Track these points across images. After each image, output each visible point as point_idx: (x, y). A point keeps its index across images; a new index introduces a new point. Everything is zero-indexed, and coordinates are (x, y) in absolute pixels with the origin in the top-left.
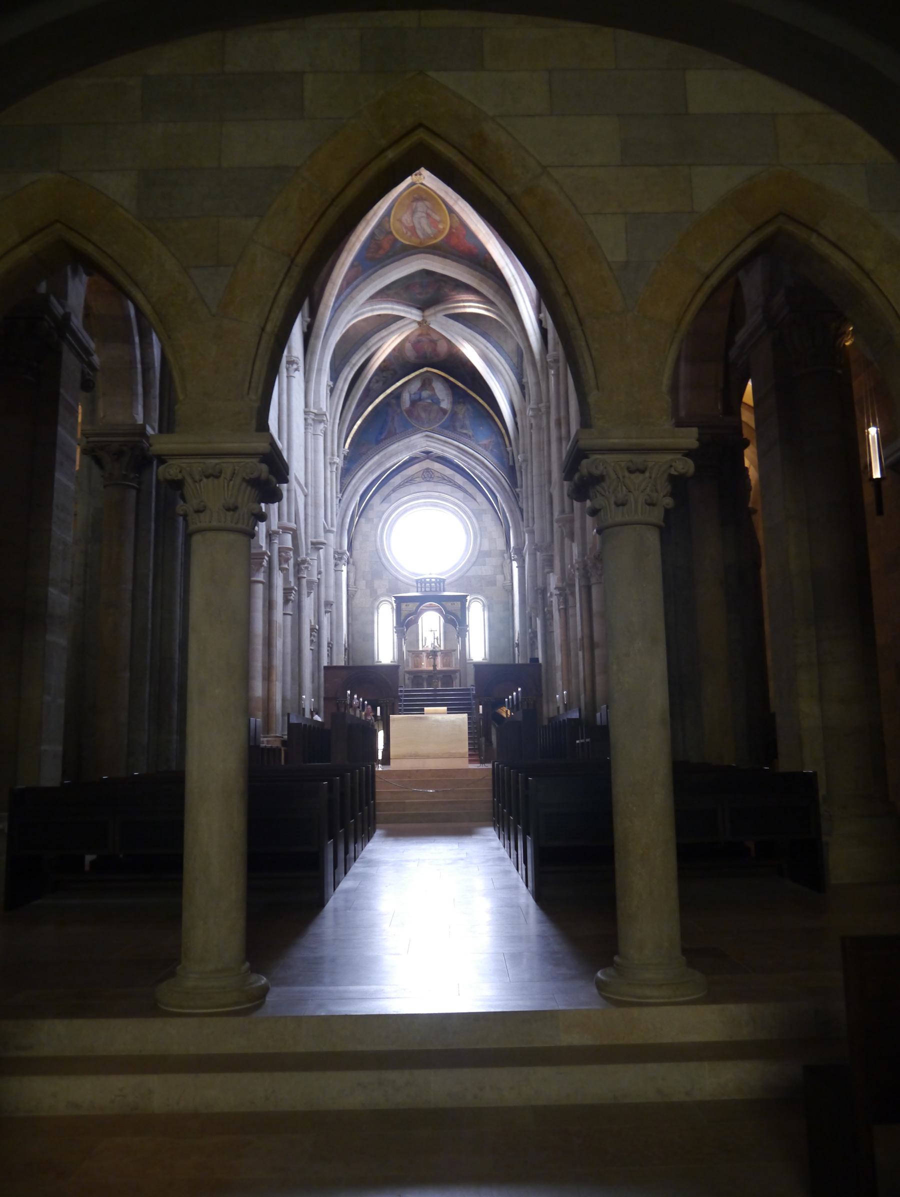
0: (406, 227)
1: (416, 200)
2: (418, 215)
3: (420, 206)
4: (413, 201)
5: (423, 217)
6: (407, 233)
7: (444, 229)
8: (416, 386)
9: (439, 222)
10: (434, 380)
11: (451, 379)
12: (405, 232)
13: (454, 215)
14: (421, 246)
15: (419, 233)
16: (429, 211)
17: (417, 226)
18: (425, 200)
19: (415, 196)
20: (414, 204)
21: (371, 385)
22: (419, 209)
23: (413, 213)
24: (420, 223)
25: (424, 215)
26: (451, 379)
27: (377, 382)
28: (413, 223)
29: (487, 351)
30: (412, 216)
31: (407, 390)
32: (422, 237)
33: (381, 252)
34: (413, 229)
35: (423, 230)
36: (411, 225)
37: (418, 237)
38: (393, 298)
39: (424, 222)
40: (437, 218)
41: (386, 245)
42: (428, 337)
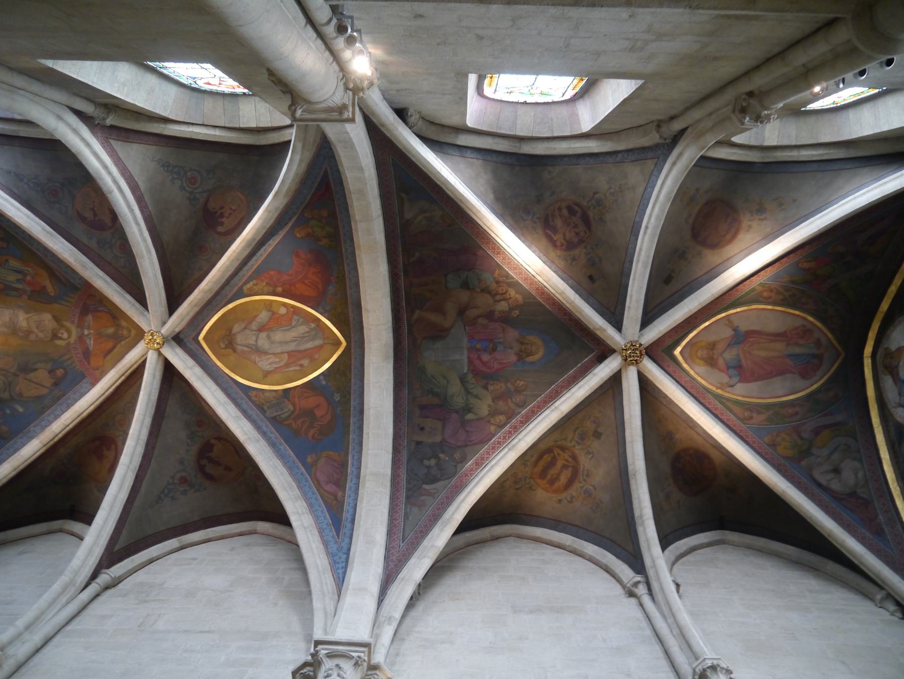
0: (287, 365)
2: (263, 341)
3: (244, 339)
4: (235, 351)
5: (269, 337)
6: (301, 366)
7: (285, 304)
8: (888, 383)
9: (274, 313)
10: (886, 346)
11: (885, 306)
12: (297, 368)
13: (245, 288)
14: (344, 344)
15: (310, 345)
16: (254, 328)
17: (292, 347)
18: (230, 330)
19: (223, 345)
20: (239, 347)
21: (835, 486)
25: (263, 335)
26: (885, 306)
27: (837, 471)
29: (650, 226)
30: (266, 353)
31: (892, 410)
32: (318, 342)
33: (319, 413)
34: (295, 356)
35: (302, 338)
36: (286, 355)
37: (320, 347)
38: (523, 405)
39: (278, 336)
40: (264, 316)
41: (311, 401)
42: (721, 347)
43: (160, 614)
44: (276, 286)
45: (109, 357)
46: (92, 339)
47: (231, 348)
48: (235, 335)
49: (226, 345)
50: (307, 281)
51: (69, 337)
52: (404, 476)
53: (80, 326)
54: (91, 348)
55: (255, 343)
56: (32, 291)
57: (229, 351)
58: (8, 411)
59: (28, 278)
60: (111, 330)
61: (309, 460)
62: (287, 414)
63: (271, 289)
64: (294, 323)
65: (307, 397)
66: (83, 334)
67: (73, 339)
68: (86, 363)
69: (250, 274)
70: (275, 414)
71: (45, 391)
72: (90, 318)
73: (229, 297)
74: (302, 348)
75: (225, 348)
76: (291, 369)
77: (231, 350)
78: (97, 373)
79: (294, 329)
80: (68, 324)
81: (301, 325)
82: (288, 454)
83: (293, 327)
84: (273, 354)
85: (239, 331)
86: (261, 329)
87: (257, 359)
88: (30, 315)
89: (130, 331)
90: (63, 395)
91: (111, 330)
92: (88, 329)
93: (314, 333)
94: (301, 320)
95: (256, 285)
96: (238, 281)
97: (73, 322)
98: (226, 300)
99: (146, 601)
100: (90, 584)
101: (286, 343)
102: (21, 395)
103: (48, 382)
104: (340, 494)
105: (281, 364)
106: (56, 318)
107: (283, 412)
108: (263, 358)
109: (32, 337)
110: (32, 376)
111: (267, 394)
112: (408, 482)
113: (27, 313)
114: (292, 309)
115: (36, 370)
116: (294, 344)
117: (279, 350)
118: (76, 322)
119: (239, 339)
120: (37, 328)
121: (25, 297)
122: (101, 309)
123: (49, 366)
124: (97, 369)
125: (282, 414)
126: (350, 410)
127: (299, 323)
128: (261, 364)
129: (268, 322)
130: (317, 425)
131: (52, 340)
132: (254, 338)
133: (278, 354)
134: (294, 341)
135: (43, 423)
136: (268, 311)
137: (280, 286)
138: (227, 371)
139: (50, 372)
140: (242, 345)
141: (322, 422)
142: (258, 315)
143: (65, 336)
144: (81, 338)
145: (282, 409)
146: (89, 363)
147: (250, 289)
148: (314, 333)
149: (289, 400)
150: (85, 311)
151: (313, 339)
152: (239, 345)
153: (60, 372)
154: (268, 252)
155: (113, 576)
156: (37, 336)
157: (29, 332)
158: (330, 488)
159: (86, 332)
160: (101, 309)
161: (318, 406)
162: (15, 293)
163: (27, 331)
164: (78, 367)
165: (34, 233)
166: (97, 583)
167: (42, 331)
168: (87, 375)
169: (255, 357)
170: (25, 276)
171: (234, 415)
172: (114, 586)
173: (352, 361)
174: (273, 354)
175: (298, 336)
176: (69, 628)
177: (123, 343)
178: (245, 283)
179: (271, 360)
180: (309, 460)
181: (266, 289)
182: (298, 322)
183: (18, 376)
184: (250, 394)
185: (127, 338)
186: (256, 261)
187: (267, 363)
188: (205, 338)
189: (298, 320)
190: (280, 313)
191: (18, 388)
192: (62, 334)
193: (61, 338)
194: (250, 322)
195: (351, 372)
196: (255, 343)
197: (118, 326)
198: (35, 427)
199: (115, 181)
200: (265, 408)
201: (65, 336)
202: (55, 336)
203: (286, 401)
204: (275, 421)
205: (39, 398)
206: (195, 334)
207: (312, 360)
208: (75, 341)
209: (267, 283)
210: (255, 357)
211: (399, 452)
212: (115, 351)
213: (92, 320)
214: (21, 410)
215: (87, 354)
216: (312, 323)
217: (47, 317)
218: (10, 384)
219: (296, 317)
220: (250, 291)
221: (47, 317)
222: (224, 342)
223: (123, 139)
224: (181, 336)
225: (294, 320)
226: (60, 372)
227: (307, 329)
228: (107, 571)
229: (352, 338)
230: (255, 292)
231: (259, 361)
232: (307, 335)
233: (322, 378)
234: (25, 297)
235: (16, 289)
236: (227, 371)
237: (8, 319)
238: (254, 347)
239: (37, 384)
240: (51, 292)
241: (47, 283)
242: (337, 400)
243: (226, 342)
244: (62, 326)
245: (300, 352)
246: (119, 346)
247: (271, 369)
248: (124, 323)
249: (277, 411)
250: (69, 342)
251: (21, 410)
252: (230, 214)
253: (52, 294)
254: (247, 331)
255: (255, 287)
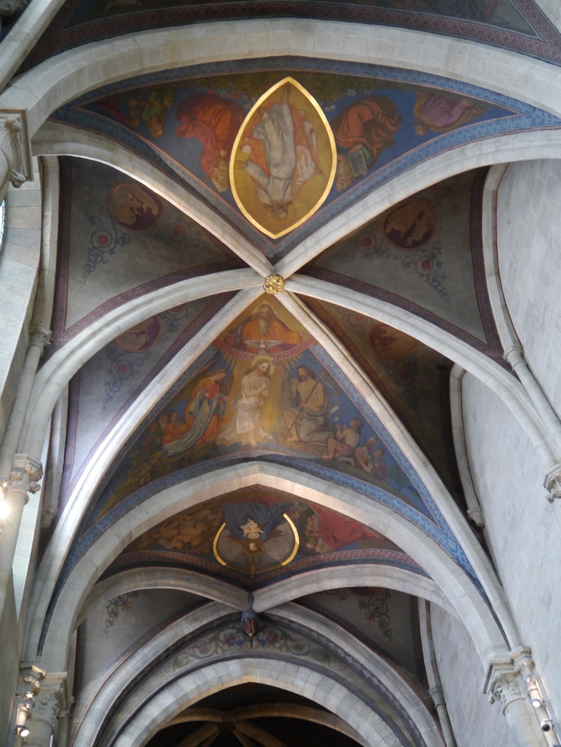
0: (310, 147)
1: (283, 206)
4: (290, 203)
5: (277, 166)
6: (312, 131)
7: (240, 147)
9: (250, 159)
12: (314, 136)
13: (220, 189)
14: (289, 79)
15: (288, 120)
16: (263, 181)
17: (289, 140)
18: (266, 206)
19: (284, 215)
20: (287, 198)
22: (281, 184)
23: (292, 177)
24: (284, 151)
25: (274, 171)
28: (296, 152)
30: (295, 169)
32: (286, 110)
33: (368, 116)
35: (279, 129)
36: (299, 147)
37: (292, 109)
39: (276, 155)
40: (253, 170)
43: (558, 314)
44: (219, 156)
45: (290, 327)
46: (270, 341)
47: (287, 206)
48: (272, 202)
49: (283, 211)
50: (214, 123)
51: (267, 361)
52: (456, 20)
53: (256, 351)
54: (279, 342)
55: (283, 181)
56: (220, 392)
57: (290, 208)
58: (337, 419)
59: (207, 395)
60: (262, 323)
61: (421, 133)
62: (367, 153)
63: (222, 162)
64: (262, 137)
65: (348, 128)
66: (264, 349)
67: (270, 359)
68: (295, 348)
69: (205, 185)
70: (364, 165)
71: (320, 386)
72: (248, 342)
73: (230, 207)
74: (291, 129)
75: (287, 212)
76: (315, 143)
77: (290, 206)
78: (304, 339)
79: (269, 137)
80: (254, 362)
81: (263, 128)
82: (412, 155)
83: (266, 137)
84: (296, 161)
85: (268, 198)
86: (268, 174)
87: (301, 179)
88: (244, 395)
89: (264, 306)
90: (325, 370)
91: (262, 323)
92: (260, 344)
93: (274, 115)
94: (259, 129)
95: (217, 178)
96: (213, 197)
97: (253, 357)
98: (234, 210)
99: (543, 324)
100: (514, 371)
101: (284, 146)
102: (321, 407)
103: (311, 383)
104: (465, 103)
105: (308, 153)
106: (248, 372)
107: (363, 155)
108: (300, 173)
109: (265, 393)
110: (303, 396)
111: (341, 173)
112: (464, 15)
113: (241, 397)
114: (246, 139)
115: (298, 392)
116: (286, 137)
117: (292, 155)
118: (251, 354)
119: (277, 197)
120: (256, 389)
121: (226, 398)
122: (239, 332)
123: (295, 381)
124: (301, 338)
125: (365, 157)
126: (368, 79)
127: (262, 130)
128: (307, 177)
129: (259, 165)
130: (381, 120)
131: (269, 377)
132: (277, 181)
133: (296, 156)
134: (283, 138)
135: (351, 390)
136: (247, 165)
137: (219, 153)
138: (312, 212)
139: (301, 380)
140: (285, 195)
141: (379, 112)
142: (252, 177)
143: (265, 365)
144: (268, 351)
145: (360, 157)
146: (295, 345)
147: (222, 185)
148: (274, 115)
149: (350, 149)
150: (242, 346)
151: (281, 115)
152: (284, 198)
153: (302, 372)
154: (180, 166)
155: (511, 349)
156: (265, 389)
157: (260, 396)
158: (456, 112)
159: (263, 346)
160: (239, 332)
161: (360, 117)
162: (221, 407)
163: (259, 398)
164: (298, 356)
165: (162, 391)
166: (515, 365)
167: (260, 385)
168: (307, 348)
169: (298, 181)
170: (205, 397)
171: (361, 209)
172: (522, 348)
173: (310, 70)
174: (296, 161)
175: (277, 134)
176: (552, 399)
177: (276, 313)
178: (215, 190)
179: (303, 164)
180: (421, 133)
181: (222, 167)
182: (261, 133)
183: (303, 408)
184: (339, 190)
185: (271, 309)
186: (190, 178)
187: (306, 169)
188: (275, 233)
189: (258, 132)
190: (249, 152)
191: (315, 409)
192: (263, 367)
193: (268, 369)
194: (259, 185)
195: (323, 74)
196: (283, 181)
197: (258, 316)
198: (354, 397)
199: (108, 324)
200: (356, 175)
201: (265, 365)
202: (266, 374)
203: (351, 151)
204: (372, 166)
205: (326, 391)
206: (269, 243)
207: (305, 118)
208: (271, 356)
209: (215, 167)
210: (298, 181)
211: (426, 22)
212: (283, 321)
213: (250, 339)
214: (336, 408)
215: (285, 347)
216: (262, 116)
217: (246, 380)
218: (310, 415)
219: (255, 135)
220: (224, 184)
221: (246, 380)
222: (280, 213)
223: (64, 314)
224: (271, 256)
225: (258, 137)
226: (302, 372)
227: (270, 122)
228: (505, 353)
229: (282, 69)
230: (225, 180)
231: (303, 177)
232: (276, 123)
233: (327, 109)
234: (226, 398)
235: (218, 405)
236: (312, 212)
237: (247, 413)
238: (288, 182)
239: (312, 392)
240: (221, 376)
241: (213, 379)
242: (355, 93)
243: (280, 211)
244: (256, 367)
245: (295, 133)
246: (279, 317)
247: (313, 166)
248: (255, 311)
249: (362, 162)
250: (272, 362)
251: (336, 408)
252: (138, 201)
253: (224, 375)
254: (269, 188)
255: (219, 180)
